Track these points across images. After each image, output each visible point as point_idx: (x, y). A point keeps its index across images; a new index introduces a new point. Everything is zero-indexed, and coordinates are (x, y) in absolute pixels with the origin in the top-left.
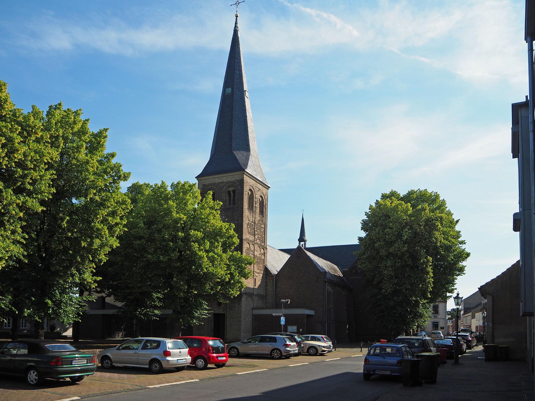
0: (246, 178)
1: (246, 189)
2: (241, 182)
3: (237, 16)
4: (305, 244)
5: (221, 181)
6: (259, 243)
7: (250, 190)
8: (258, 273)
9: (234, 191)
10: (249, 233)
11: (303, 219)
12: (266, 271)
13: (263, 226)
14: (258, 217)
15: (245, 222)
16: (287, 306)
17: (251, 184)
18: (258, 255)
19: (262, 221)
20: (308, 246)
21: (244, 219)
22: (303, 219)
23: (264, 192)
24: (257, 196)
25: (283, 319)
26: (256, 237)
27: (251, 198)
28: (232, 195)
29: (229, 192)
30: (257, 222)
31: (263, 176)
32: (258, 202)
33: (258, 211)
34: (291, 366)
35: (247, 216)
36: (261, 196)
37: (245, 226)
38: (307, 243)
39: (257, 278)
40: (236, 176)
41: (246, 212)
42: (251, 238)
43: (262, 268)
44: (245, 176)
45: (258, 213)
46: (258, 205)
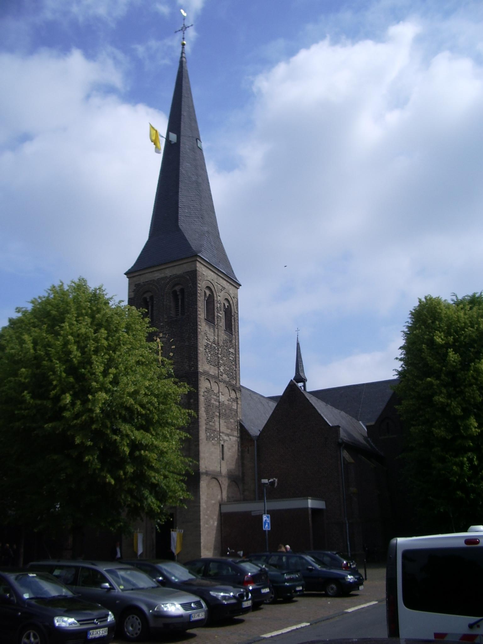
0: (202, 269)
1: (202, 285)
2: (193, 275)
3: (176, 32)
4: (304, 386)
5: (163, 275)
6: (227, 379)
7: (208, 288)
8: (228, 435)
9: (182, 291)
10: (209, 362)
11: (298, 344)
12: (243, 432)
13: (232, 350)
14: (223, 336)
15: (202, 342)
16: (273, 493)
17: (209, 278)
18: (226, 402)
19: (231, 341)
20: (309, 388)
21: (200, 337)
22: (298, 344)
23: (231, 292)
24: (220, 298)
25: (266, 518)
26: (222, 369)
27: (210, 301)
28: (180, 297)
29: (175, 293)
30: (221, 343)
31: (236, 279)
32: (222, 309)
33: (222, 323)
34: (268, 635)
35: (206, 334)
36: (227, 299)
37: (201, 349)
38: (307, 383)
39: (225, 445)
40: (185, 266)
41: (203, 327)
42: (213, 371)
43: (235, 426)
44: (198, 264)
45: (224, 328)
46: (222, 314)
